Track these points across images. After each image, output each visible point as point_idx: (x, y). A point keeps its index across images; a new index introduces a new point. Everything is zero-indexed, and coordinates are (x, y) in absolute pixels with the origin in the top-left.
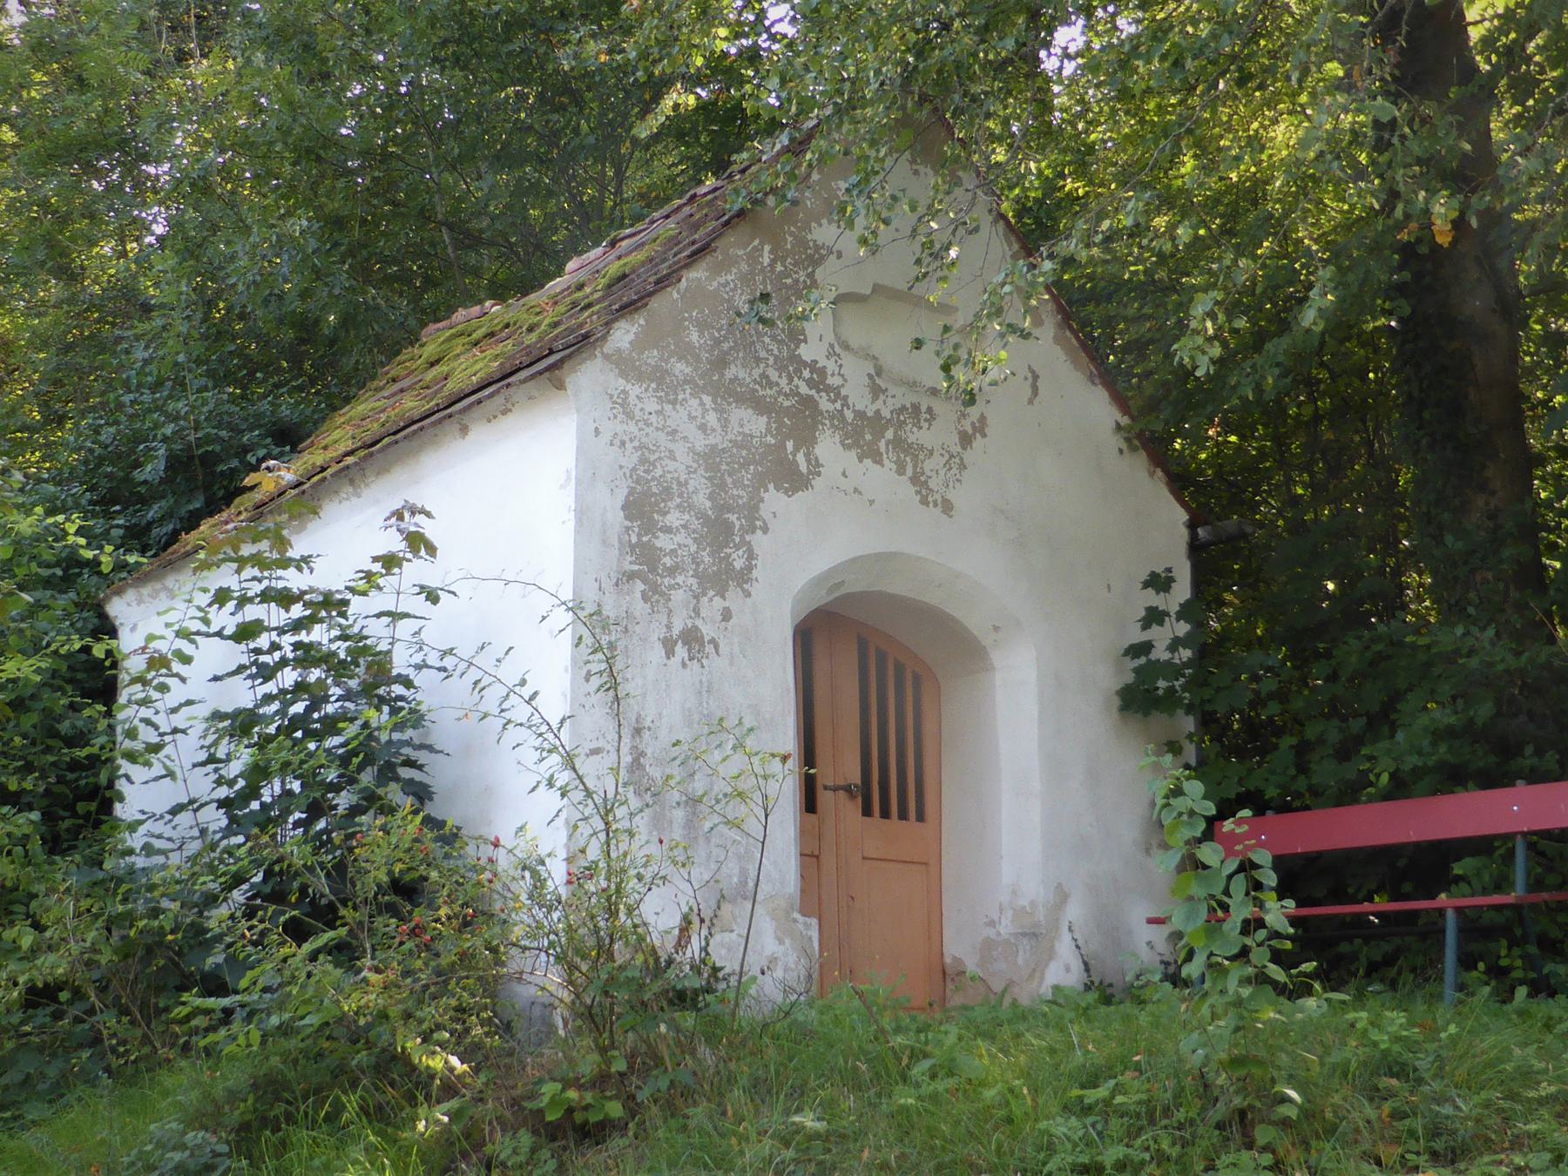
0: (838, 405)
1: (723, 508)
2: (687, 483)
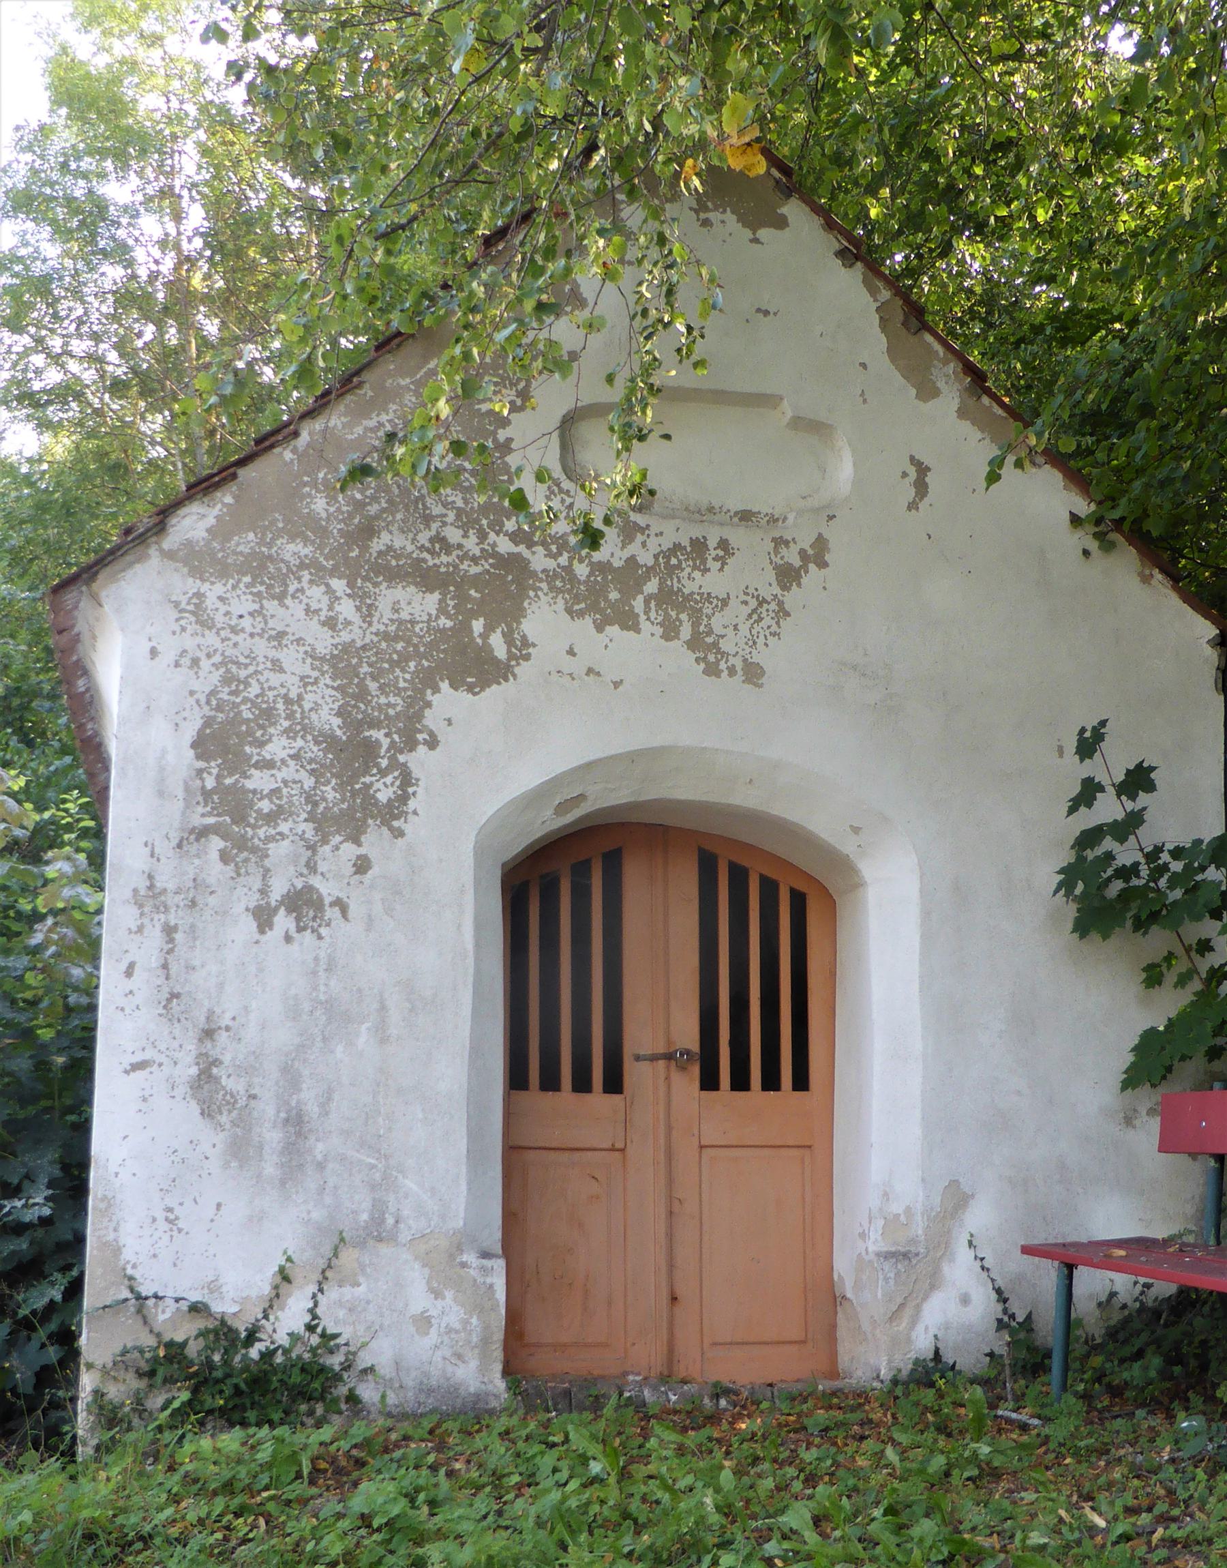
0: (563, 560)
1: (355, 725)
2: (300, 697)
